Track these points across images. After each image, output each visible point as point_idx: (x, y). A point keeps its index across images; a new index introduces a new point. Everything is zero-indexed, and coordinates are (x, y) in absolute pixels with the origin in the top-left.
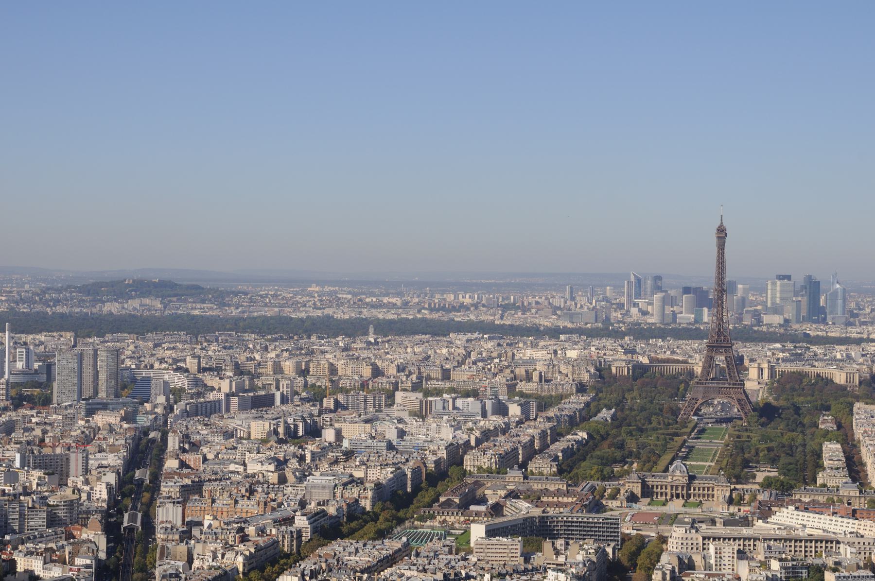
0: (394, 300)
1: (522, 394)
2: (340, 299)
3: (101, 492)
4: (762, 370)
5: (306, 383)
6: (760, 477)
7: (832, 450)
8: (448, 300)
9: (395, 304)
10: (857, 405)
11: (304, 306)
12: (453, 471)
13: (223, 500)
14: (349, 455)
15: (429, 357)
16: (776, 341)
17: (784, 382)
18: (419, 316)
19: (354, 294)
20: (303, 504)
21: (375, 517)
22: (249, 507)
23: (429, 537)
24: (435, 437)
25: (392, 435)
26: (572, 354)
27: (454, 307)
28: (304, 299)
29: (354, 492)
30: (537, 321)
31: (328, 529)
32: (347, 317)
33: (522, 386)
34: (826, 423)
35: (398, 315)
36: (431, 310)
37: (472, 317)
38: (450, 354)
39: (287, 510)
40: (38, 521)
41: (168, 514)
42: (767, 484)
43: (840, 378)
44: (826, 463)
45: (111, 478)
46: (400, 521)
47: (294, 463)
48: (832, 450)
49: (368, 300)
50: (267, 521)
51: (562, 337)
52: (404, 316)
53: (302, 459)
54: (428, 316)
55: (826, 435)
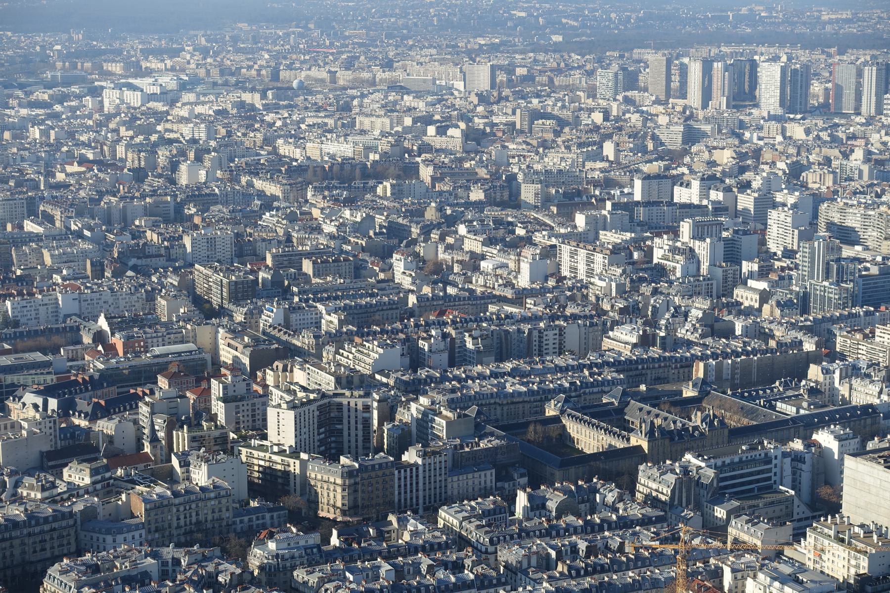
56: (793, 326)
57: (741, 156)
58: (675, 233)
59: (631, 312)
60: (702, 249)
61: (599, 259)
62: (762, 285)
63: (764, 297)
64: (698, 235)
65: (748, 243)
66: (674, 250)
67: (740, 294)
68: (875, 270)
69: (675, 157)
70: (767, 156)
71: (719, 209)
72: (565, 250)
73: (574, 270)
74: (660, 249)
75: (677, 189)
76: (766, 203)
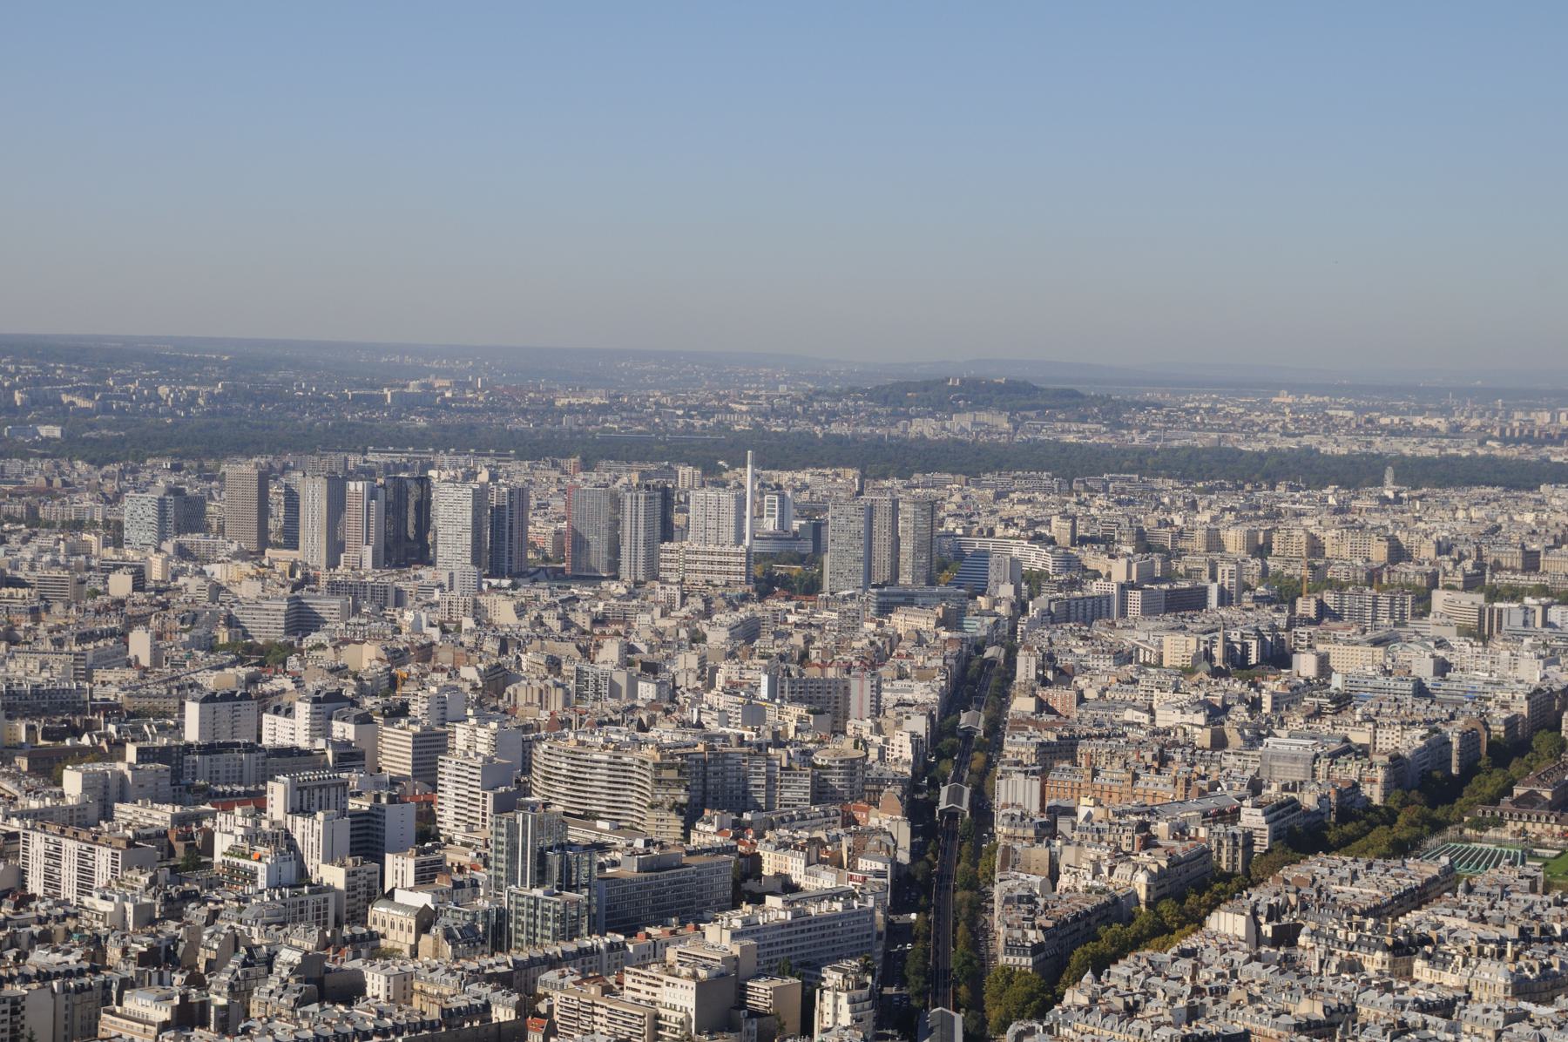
0: (1433, 422)
2: (1331, 418)
3: (902, 749)
5: (1265, 569)
8: (1538, 423)
9: (1434, 431)
11: (1265, 430)
12: (1542, 740)
13: (1113, 773)
14: (1342, 702)
15: (1499, 528)
18: (1480, 452)
19: (1359, 411)
20: (1256, 787)
21: (1388, 817)
22: (1159, 787)
23: (1493, 860)
24: (1508, 676)
25: (1424, 669)
27: (1549, 436)
28: (1266, 417)
29: (1351, 770)
31: (1301, 834)
32: (1343, 451)
35: (1441, 449)
36: (1505, 441)
38: (1540, 523)
39: (1227, 795)
40: (797, 792)
41: (1015, 793)
45: (919, 725)
46: (1438, 827)
47: (1240, 713)
49: (1385, 421)
50: (1191, 812)
52: (1453, 451)
53: (1255, 705)
54: (1498, 453)
56: (477, 976)
57: (397, 657)
58: (258, 802)
59: (160, 959)
60: (309, 832)
61: (103, 859)
62: (423, 899)
63: (425, 921)
64: (300, 808)
65: (400, 820)
66: (253, 836)
67: (378, 911)
68: (630, 870)
69: (268, 657)
70: (444, 657)
71: (349, 756)
72: (38, 844)
73: (51, 880)
74: (227, 832)
75: (267, 719)
76: (430, 748)
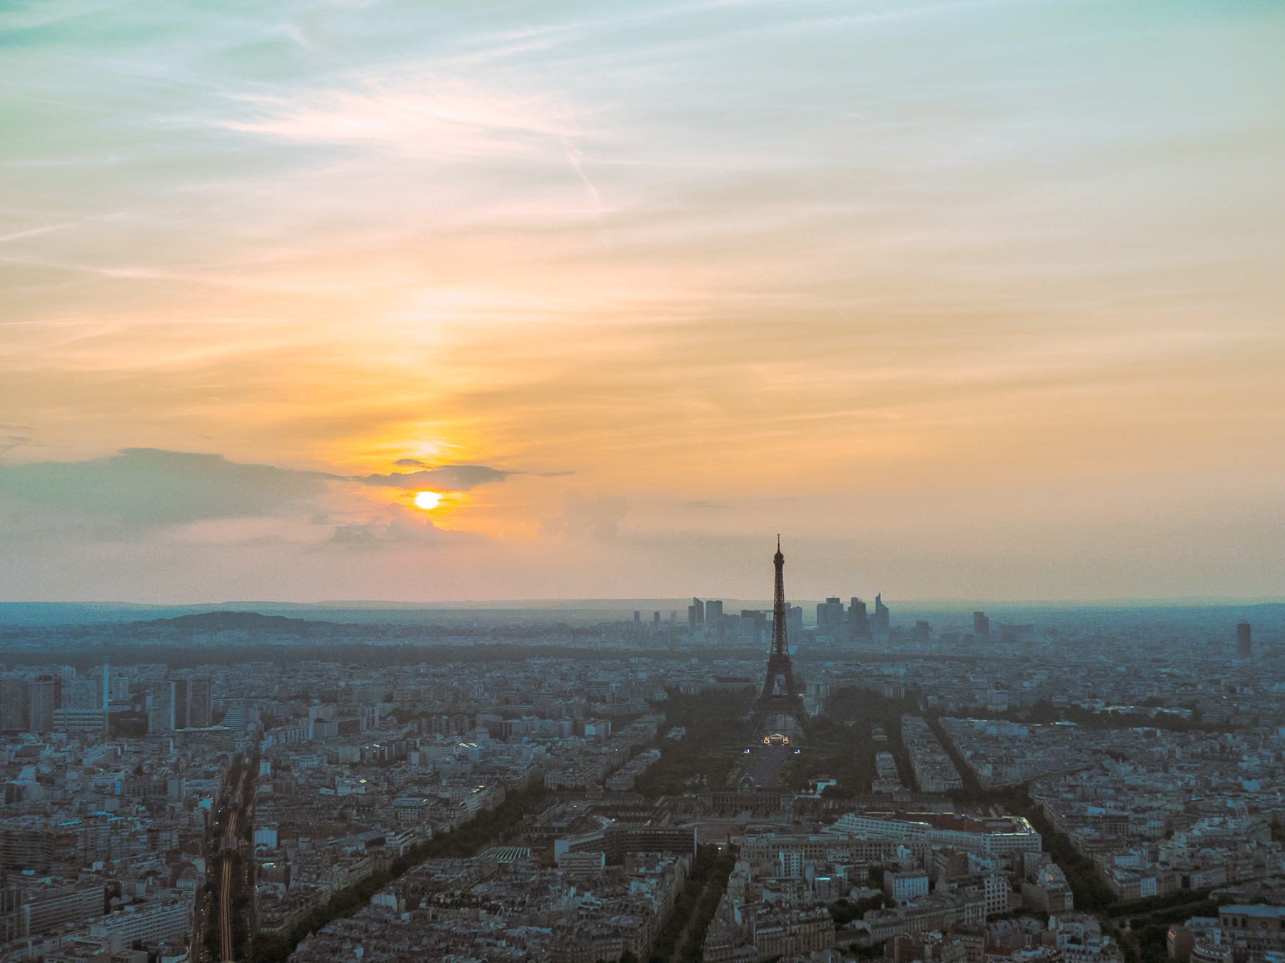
1: (594, 715)
4: (818, 687)
6: (821, 786)
7: (885, 760)
10: (905, 717)
16: (829, 659)
17: (841, 698)
26: (642, 676)
30: (608, 645)
33: (600, 707)
34: (880, 736)
37: (546, 643)
42: (828, 793)
43: (889, 692)
44: (880, 772)
48: (885, 760)
51: (633, 660)
55: (882, 747)
